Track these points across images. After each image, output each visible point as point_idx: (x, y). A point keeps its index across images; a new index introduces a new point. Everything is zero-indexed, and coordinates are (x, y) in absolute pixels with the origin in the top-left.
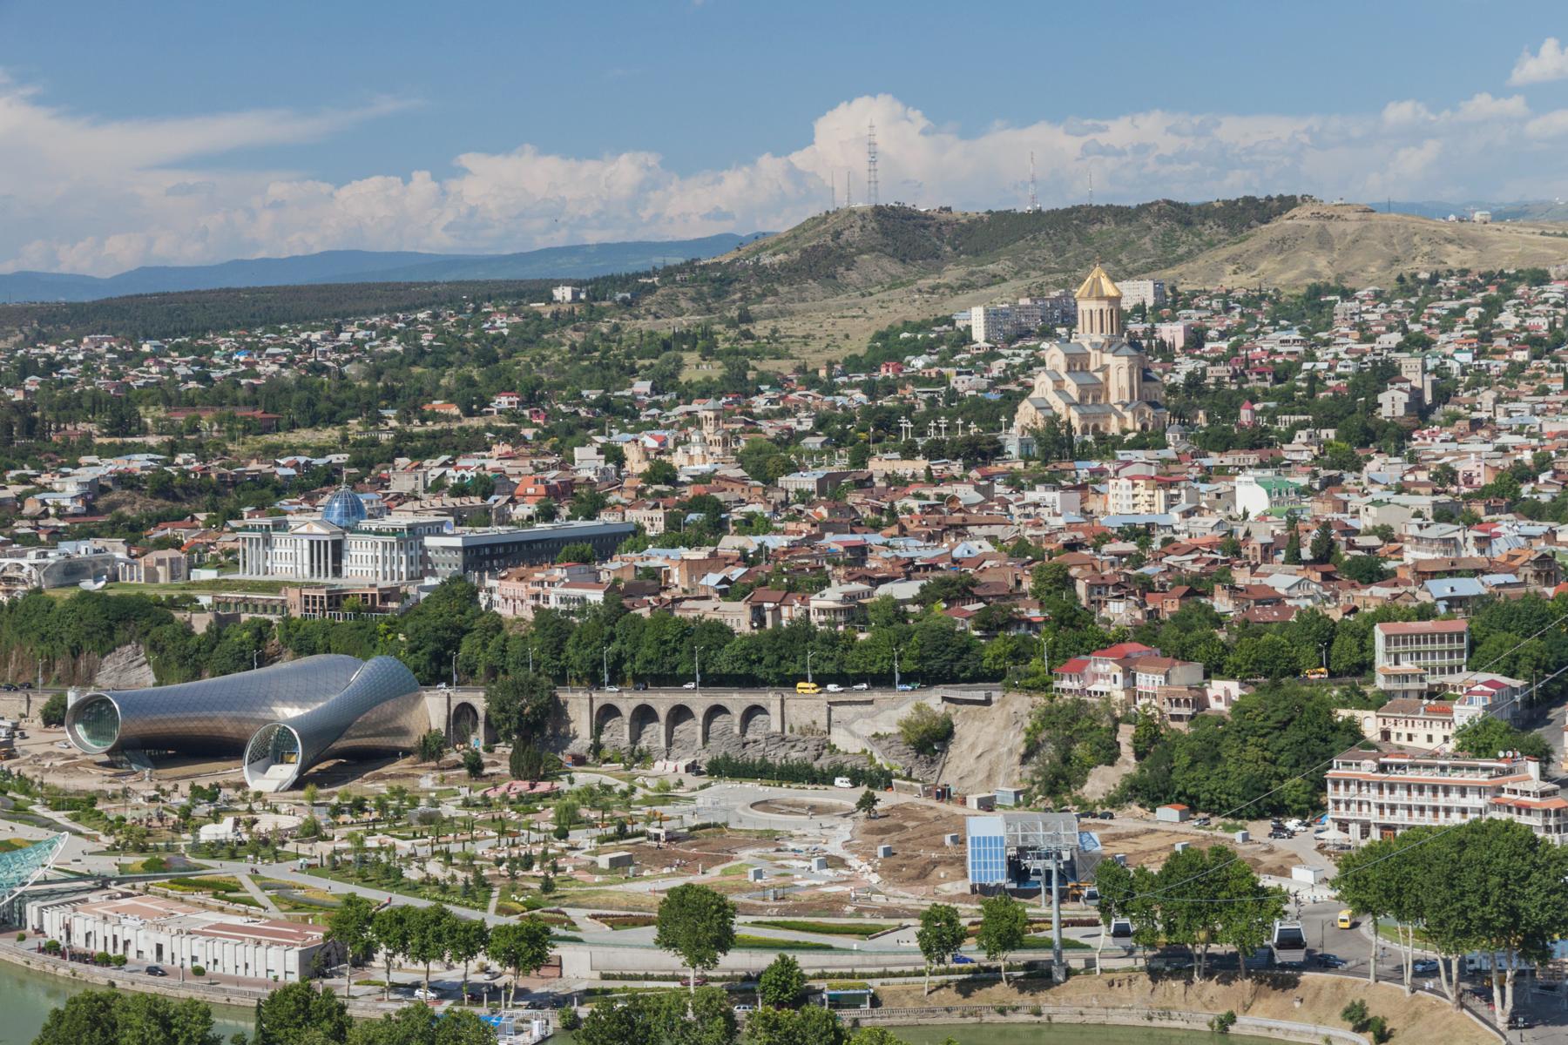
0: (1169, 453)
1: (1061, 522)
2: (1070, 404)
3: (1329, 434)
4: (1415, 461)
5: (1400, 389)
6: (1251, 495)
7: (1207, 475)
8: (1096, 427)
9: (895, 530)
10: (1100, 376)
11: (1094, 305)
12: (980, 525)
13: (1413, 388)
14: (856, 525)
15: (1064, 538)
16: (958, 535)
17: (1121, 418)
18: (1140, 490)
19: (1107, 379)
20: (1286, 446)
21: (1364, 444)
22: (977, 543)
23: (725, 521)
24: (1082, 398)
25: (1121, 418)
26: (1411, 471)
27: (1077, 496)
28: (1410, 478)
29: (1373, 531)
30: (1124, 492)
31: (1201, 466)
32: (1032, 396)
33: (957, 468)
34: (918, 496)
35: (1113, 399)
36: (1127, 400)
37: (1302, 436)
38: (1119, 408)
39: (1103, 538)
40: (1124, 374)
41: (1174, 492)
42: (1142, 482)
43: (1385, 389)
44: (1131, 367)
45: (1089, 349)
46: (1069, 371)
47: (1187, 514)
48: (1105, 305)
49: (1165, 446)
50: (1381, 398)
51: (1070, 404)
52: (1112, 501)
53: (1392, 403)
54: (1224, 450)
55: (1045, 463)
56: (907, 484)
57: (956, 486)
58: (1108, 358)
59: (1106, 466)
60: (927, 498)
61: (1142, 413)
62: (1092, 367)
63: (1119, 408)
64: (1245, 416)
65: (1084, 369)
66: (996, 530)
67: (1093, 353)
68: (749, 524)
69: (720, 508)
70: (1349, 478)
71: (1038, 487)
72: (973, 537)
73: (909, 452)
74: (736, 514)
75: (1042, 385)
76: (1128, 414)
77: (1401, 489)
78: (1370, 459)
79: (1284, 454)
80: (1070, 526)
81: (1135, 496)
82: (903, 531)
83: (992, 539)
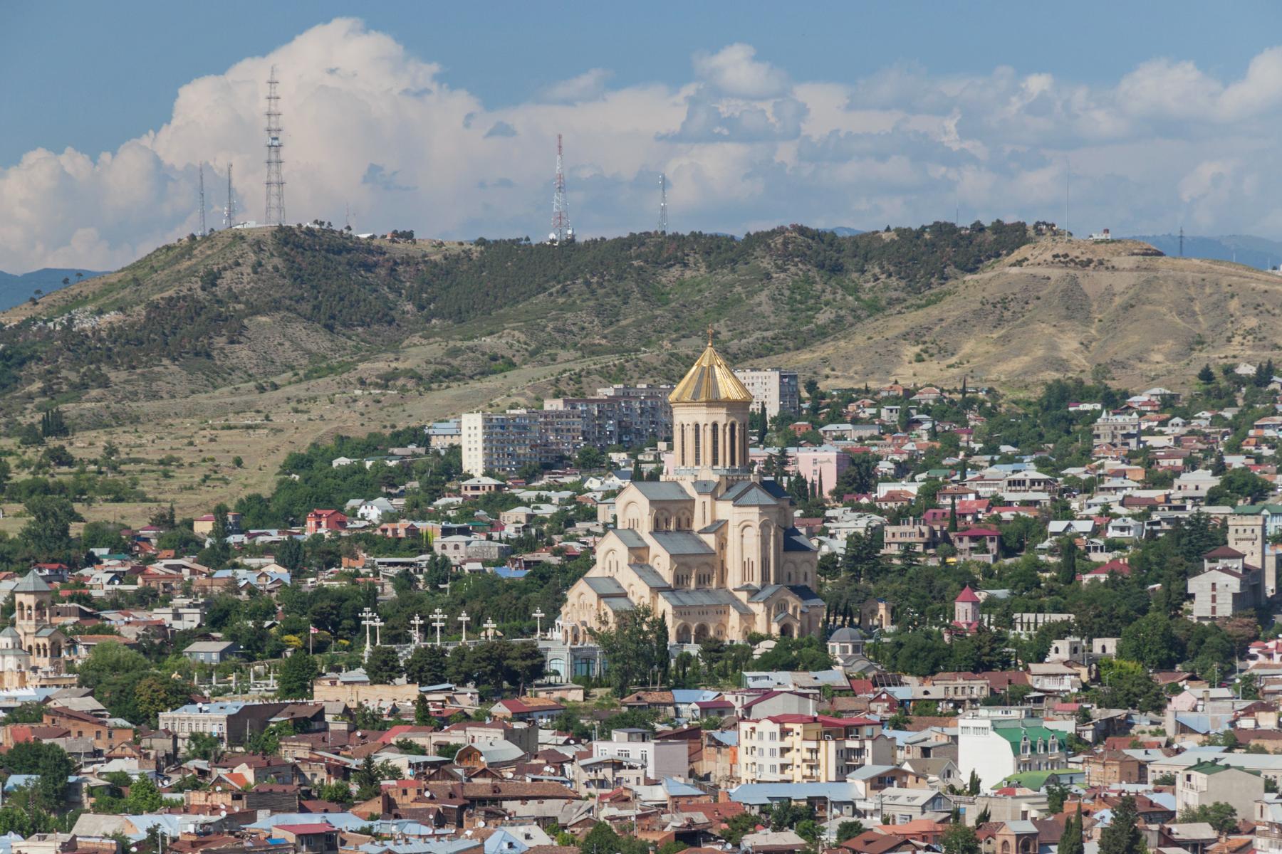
0: (835, 677)
1: (660, 794)
2: (657, 590)
3: (1107, 646)
4: (1250, 689)
5: (1226, 570)
6: (984, 750)
7: (903, 715)
8: (702, 630)
9: (376, 806)
10: (710, 540)
11: (703, 416)
12: (524, 799)
13: (1247, 569)
14: (305, 799)
15: (675, 822)
16: (490, 815)
17: (747, 615)
18: (794, 740)
19: (722, 545)
20: (1034, 667)
21: (1166, 665)
22: (522, 829)
23: (76, 787)
24: (680, 579)
25: (747, 615)
26: (1248, 712)
27: (681, 750)
28: (1246, 723)
29: (1201, 815)
30: (767, 744)
31: (891, 699)
32: (593, 573)
33: (467, 699)
34: (406, 747)
35: (734, 580)
36: (756, 582)
37: (1062, 648)
38: (743, 596)
39: (741, 823)
40: (752, 539)
41: (852, 744)
42: (797, 728)
43: (1198, 571)
44: (764, 526)
45: (692, 492)
46: (657, 530)
47: (879, 783)
48: (721, 416)
49: (828, 665)
50: (1193, 585)
51: (657, 590)
52: (743, 758)
53: (1211, 594)
54: (929, 672)
55: (622, 691)
56: (384, 727)
57: (472, 731)
58: (725, 510)
59: (729, 698)
60: (423, 752)
61: (782, 607)
62: (697, 525)
63: (743, 596)
64: (963, 612)
65: (684, 527)
66: (551, 807)
67: (699, 500)
68: (115, 795)
69: (65, 764)
70: (1142, 722)
71: (616, 734)
72: (515, 821)
73: (383, 671)
74: (92, 776)
75: (611, 557)
76: (758, 609)
77: (1234, 741)
78: (1178, 690)
79: (1031, 680)
80: (678, 802)
81: (784, 751)
82: (391, 809)
83: (548, 823)
